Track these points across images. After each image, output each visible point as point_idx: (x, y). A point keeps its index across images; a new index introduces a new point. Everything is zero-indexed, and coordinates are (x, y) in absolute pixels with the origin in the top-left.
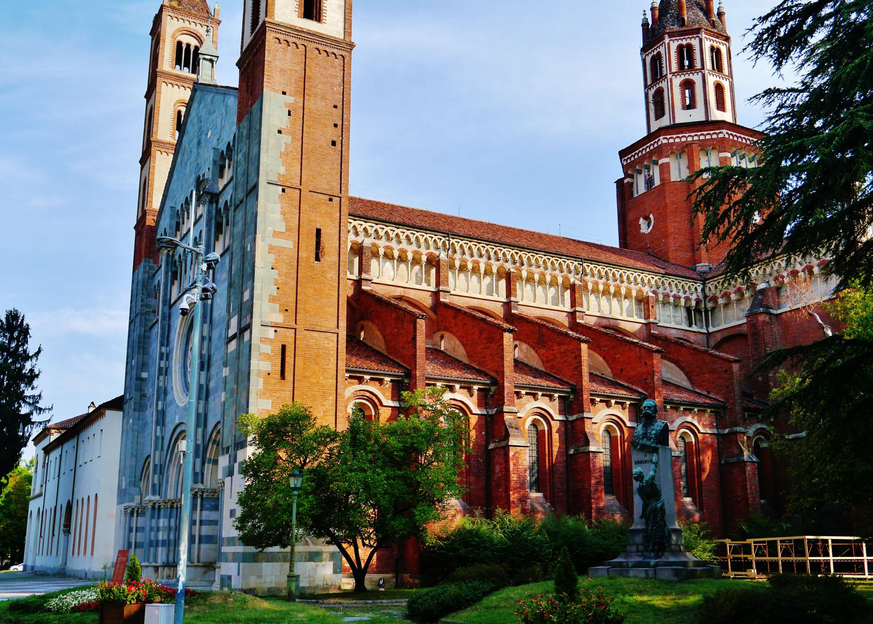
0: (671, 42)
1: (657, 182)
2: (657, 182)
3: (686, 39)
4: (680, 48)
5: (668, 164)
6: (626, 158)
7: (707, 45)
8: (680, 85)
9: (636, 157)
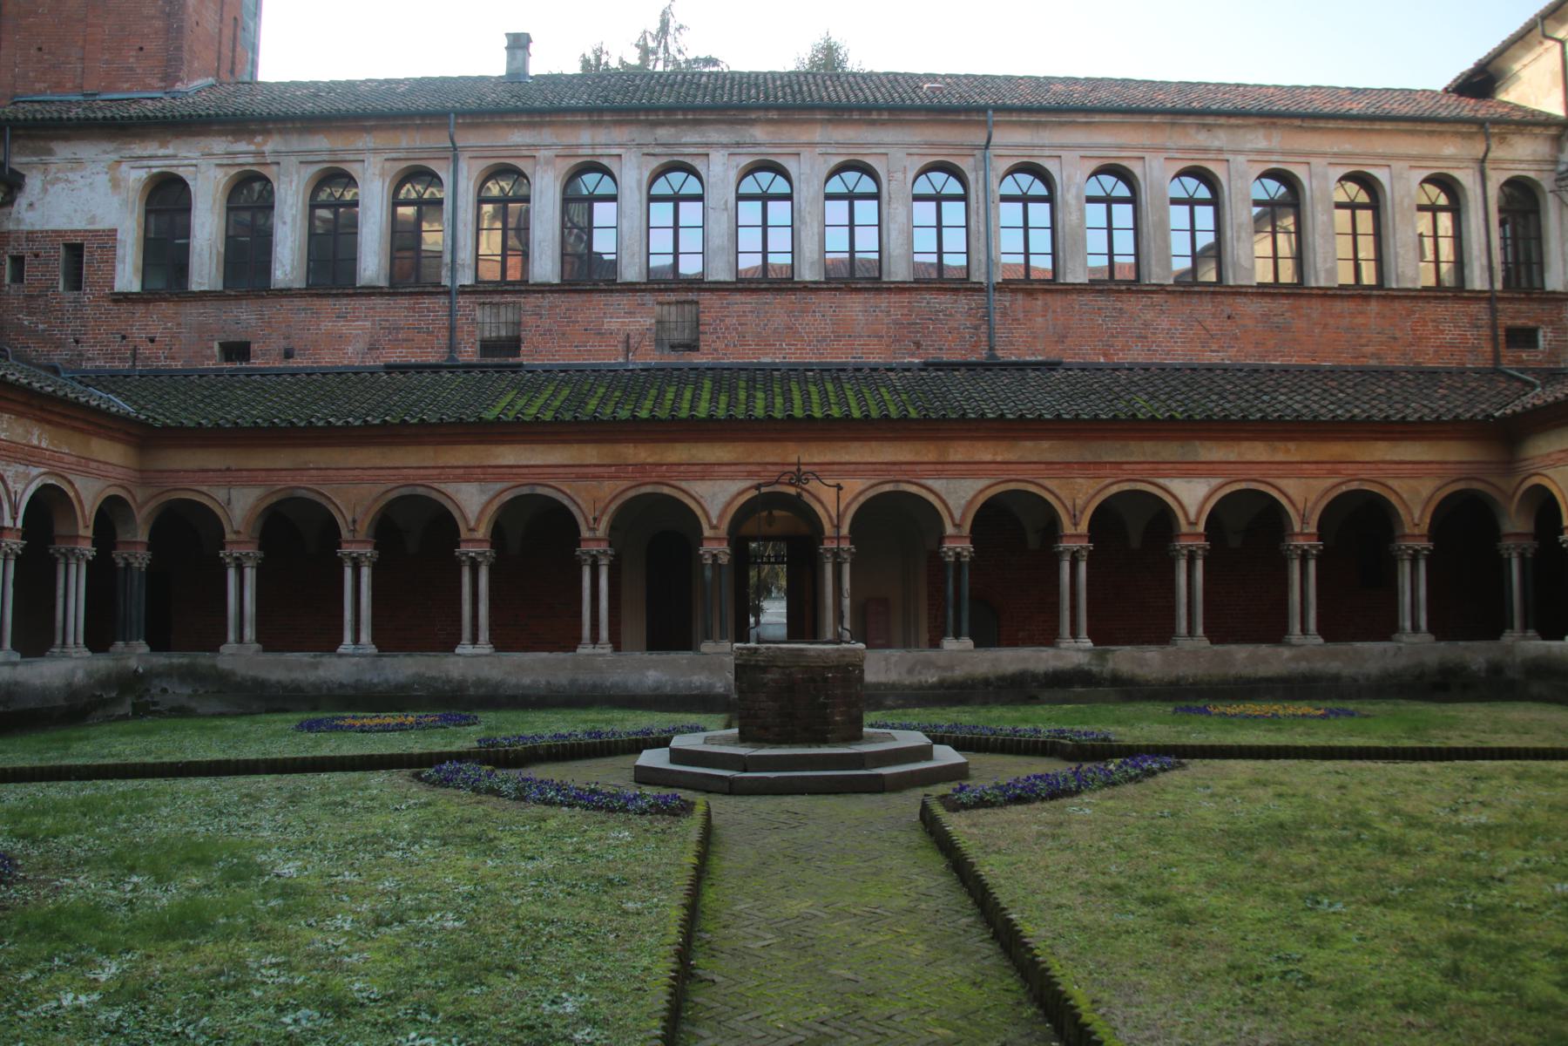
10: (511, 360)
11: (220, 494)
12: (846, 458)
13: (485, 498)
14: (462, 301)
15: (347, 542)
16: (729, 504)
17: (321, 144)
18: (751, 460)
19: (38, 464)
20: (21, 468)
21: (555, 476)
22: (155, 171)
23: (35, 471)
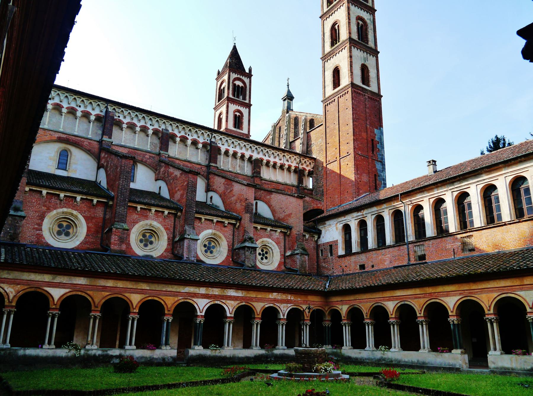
10: (424, 261)
11: (340, 307)
12: (489, 286)
13: (394, 305)
14: (410, 246)
15: (366, 319)
16: (455, 304)
17: (375, 209)
18: (460, 289)
19: (290, 303)
20: (285, 305)
21: (410, 298)
22: (344, 224)
23: (289, 305)
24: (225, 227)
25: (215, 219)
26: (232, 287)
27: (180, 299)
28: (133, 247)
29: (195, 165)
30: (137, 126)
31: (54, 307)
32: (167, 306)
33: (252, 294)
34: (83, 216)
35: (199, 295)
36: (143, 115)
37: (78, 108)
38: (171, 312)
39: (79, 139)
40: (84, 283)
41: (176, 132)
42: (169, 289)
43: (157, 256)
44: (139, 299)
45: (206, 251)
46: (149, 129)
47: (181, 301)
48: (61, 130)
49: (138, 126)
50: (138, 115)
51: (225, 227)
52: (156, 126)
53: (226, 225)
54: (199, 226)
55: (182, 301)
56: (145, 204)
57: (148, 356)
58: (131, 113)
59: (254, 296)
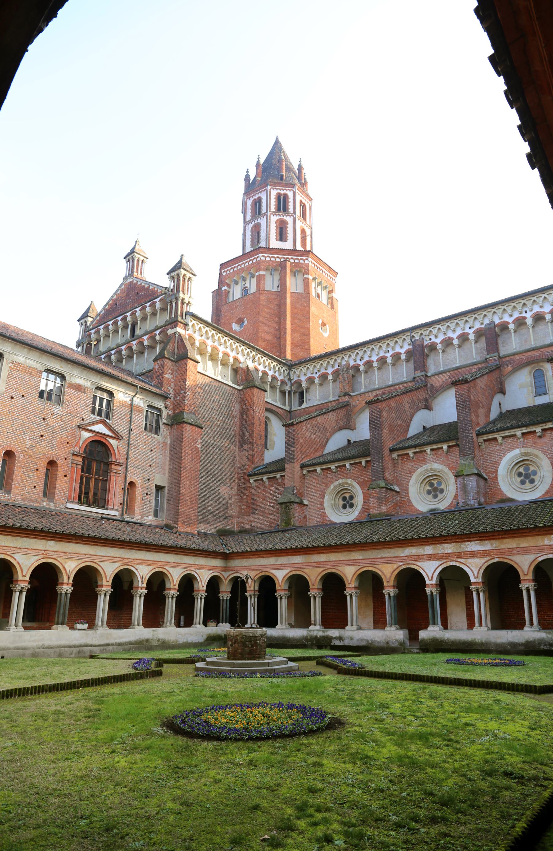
0: (272, 190)
1: (253, 289)
2: (253, 289)
3: (283, 190)
4: (278, 196)
5: (264, 276)
6: (226, 270)
7: (298, 198)
8: (276, 222)
9: (235, 269)
24: (540, 437)
25: (519, 432)
26: (471, 538)
27: (400, 566)
28: (414, 504)
29: (545, 350)
30: (453, 339)
31: (279, 588)
32: (386, 577)
33: (510, 543)
34: (358, 483)
35: (425, 557)
36: (456, 321)
37: (386, 355)
38: (391, 583)
39: (395, 387)
40: (300, 562)
41: (507, 318)
42: (385, 556)
43: (445, 507)
44: (354, 572)
45: (523, 483)
46: (468, 334)
47: (401, 568)
48: (376, 387)
49: (455, 338)
50: (449, 325)
51: (540, 437)
52: (477, 326)
53: (539, 434)
54: (498, 450)
55: (403, 567)
56: (415, 446)
57: (369, 639)
58: (441, 327)
59: (515, 546)
